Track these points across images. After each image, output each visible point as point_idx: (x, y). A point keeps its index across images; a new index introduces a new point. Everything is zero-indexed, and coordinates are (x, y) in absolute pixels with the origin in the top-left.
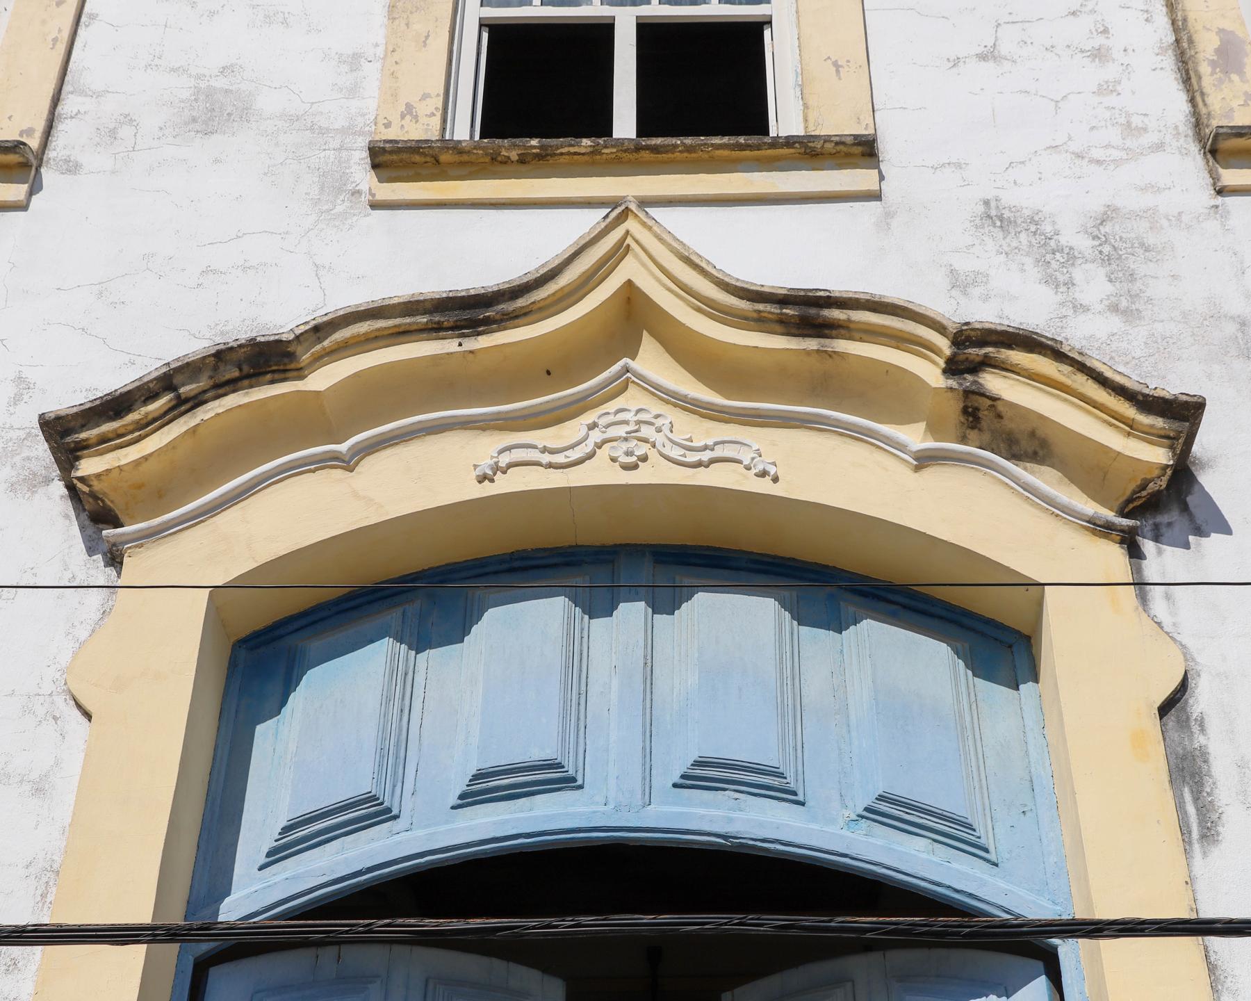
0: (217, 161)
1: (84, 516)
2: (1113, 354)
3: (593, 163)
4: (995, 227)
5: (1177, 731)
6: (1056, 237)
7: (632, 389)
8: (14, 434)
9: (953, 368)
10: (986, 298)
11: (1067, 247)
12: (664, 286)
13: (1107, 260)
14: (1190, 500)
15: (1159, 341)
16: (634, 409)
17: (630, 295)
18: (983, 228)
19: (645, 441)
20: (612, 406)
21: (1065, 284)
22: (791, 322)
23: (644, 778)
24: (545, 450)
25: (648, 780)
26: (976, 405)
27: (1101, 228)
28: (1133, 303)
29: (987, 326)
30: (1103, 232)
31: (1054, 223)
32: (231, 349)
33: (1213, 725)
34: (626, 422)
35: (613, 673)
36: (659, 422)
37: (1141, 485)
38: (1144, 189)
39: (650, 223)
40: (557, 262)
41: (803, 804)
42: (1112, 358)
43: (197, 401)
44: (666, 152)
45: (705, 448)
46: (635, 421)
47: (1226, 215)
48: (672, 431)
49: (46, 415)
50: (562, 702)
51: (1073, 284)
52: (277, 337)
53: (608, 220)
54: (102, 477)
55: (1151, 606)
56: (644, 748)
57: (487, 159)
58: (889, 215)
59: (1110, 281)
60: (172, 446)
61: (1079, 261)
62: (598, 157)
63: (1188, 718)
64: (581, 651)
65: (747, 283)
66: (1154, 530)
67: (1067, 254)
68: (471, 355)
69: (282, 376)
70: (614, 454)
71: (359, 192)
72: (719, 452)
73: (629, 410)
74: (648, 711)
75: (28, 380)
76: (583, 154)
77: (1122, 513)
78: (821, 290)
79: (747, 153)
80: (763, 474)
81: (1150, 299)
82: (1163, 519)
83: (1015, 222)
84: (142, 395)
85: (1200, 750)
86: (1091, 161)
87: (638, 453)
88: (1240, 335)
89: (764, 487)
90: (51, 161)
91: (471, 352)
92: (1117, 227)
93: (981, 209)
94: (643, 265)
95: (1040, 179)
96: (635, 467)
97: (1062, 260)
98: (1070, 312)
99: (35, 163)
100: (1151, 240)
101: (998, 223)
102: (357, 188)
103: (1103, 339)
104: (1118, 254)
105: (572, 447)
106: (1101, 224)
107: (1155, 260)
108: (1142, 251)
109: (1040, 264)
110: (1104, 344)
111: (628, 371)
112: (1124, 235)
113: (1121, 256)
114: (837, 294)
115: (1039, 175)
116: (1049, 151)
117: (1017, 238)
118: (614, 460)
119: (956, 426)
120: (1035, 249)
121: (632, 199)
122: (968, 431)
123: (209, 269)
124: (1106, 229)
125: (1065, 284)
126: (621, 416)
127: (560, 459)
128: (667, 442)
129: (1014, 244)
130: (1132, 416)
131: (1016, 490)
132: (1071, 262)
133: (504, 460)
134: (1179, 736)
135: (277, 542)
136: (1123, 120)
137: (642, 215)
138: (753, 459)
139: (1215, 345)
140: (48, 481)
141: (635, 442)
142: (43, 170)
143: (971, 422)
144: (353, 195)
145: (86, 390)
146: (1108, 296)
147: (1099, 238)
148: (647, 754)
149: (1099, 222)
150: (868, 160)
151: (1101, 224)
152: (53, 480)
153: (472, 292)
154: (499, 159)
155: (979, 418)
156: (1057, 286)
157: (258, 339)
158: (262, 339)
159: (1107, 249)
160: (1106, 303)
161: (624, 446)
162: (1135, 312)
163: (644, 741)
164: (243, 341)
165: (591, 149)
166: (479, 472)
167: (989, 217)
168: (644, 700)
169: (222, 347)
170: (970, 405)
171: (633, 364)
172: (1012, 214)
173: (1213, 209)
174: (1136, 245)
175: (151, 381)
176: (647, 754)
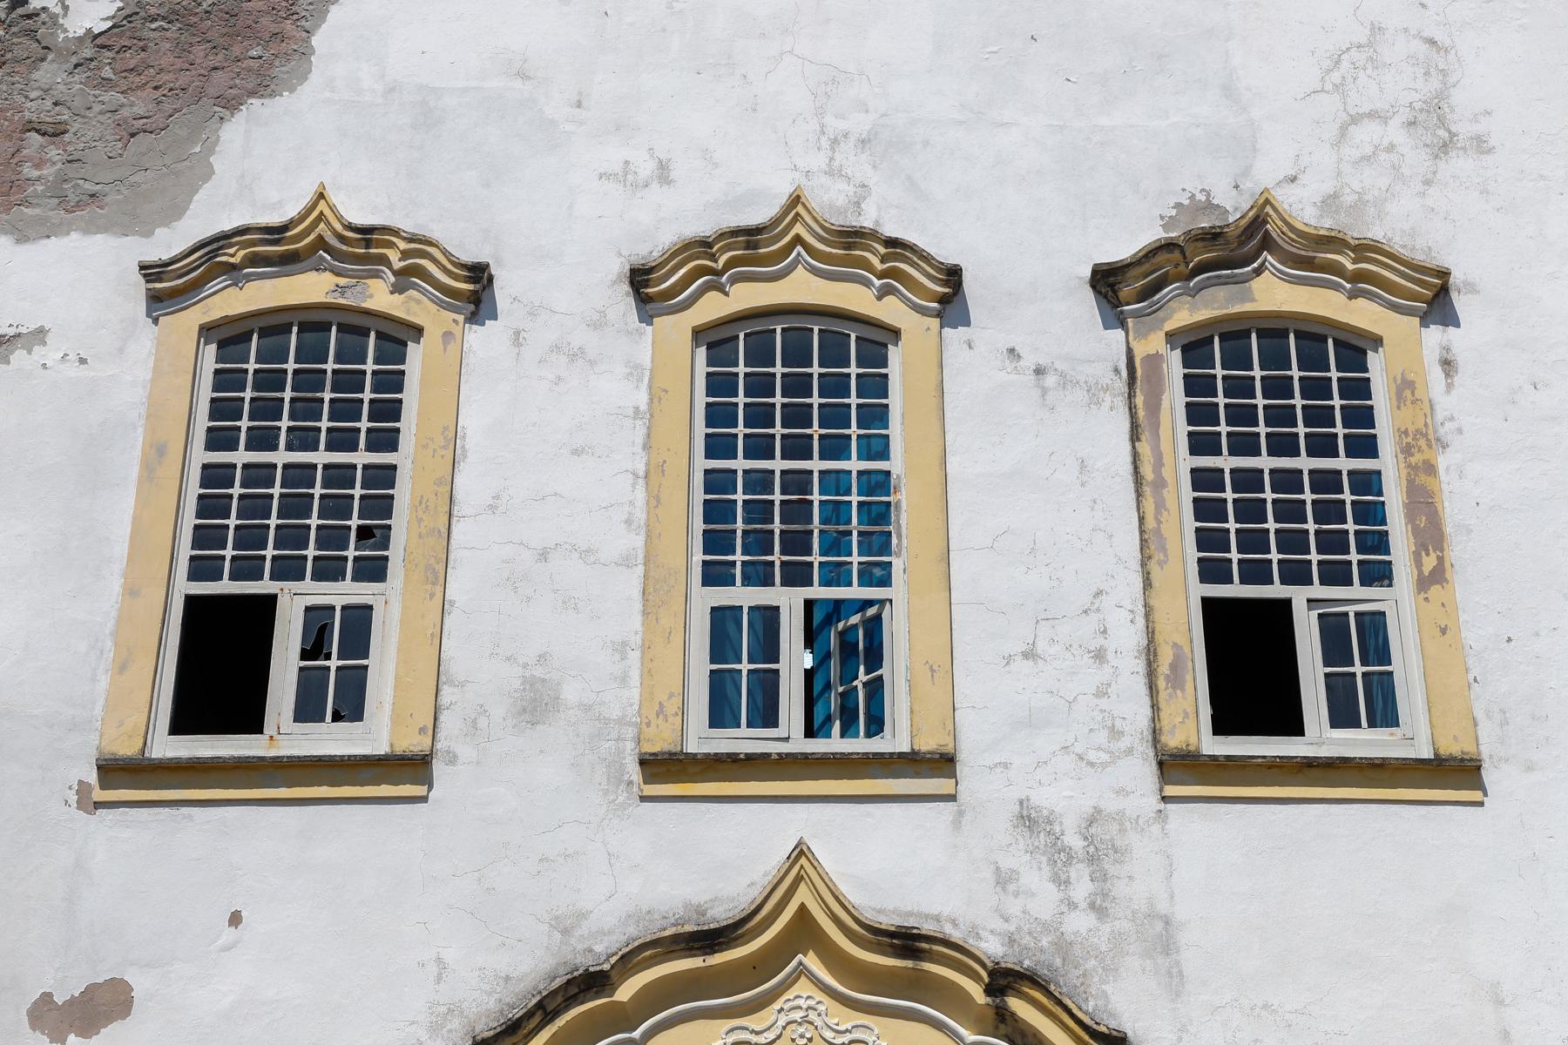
2: (1089, 949)
7: (803, 978)
10: (1016, 895)
12: (823, 909)
13: (1092, 860)
16: (805, 996)
20: (789, 995)
24: (753, 1032)
28: (1104, 901)
34: (800, 1007)
36: (822, 1008)
45: (847, 1031)
51: (1070, 883)
58: (961, 813)
70: (794, 1037)
73: (802, 997)
87: (808, 1035)
94: (811, 891)
97: (1064, 860)
98: (1065, 909)
100: (1118, 843)
101: (1027, 824)
105: (769, 1028)
113: (1099, 856)
124: (1093, 830)
128: (825, 1027)
129: (1036, 844)
136: (1109, 723)
138: (874, 1042)
146: (1089, 894)
147: (1088, 839)
149: (1088, 823)
160: (1088, 900)
161: (801, 1030)
162: (1105, 910)
167: (1022, 817)
171: (806, 961)
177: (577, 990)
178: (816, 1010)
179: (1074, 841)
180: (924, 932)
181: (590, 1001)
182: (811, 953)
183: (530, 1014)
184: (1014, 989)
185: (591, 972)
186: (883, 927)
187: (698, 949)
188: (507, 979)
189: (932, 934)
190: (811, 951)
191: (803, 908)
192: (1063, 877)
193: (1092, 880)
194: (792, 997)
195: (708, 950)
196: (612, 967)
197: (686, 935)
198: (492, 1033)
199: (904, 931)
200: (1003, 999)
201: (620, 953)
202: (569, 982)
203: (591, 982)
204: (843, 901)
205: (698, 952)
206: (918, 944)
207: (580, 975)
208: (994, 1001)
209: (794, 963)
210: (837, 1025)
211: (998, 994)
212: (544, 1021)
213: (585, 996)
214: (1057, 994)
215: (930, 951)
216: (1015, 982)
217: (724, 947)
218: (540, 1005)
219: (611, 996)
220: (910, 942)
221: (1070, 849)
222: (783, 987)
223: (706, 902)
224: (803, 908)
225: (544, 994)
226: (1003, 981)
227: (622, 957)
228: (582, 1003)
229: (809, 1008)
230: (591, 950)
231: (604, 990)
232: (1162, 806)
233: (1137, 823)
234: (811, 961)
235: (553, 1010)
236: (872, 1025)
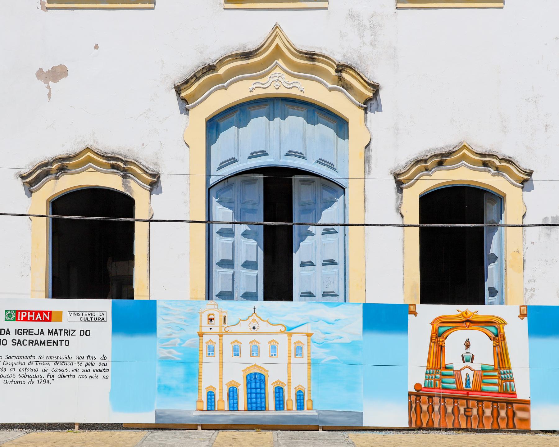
9: (337, 71)
13: (372, 29)
14: (378, 97)
16: (278, 73)
20: (273, 72)
36: (282, 76)
41: (306, 159)
45: (291, 84)
61: (366, 29)
80: (301, 91)
82: (372, 102)
89: (301, 94)
94: (280, 39)
96: (278, 88)
118: (274, 86)
124: (372, 19)
125: (363, 36)
127: (264, 86)
133: (255, 86)
161: (277, 83)
167: (350, 15)
177: (206, 71)
178: (281, 77)
179: (367, 23)
180: (316, 53)
181: (210, 74)
182: (280, 60)
183: (192, 78)
184: (344, 71)
186: (303, 51)
187: (244, 58)
188: (184, 67)
189: (319, 53)
190: (280, 59)
191: (277, 45)
192: (362, 35)
193: (371, 36)
194: (274, 73)
195: (247, 58)
196: (217, 63)
198: (180, 83)
199: (310, 52)
200: (341, 74)
201: (219, 59)
202: (203, 68)
203: (211, 68)
204: (290, 43)
205: (244, 59)
206: (314, 56)
207: (207, 66)
208: (338, 74)
209: (275, 63)
210: (288, 82)
211: (339, 72)
214: (358, 72)
215: (318, 59)
218: (195, 75)
220: (312, 56)
221: (365, 25)
222: (271, 70)
223: (246, 43)
224: (277, 45)
225: (196, 72)
226: (341, 68)
227: (220, 60)
228: (208, 75)
229: (279, 77)
230: (210, 58)
232: (396, 10)
233: (387, 17)
234: (280, 62)
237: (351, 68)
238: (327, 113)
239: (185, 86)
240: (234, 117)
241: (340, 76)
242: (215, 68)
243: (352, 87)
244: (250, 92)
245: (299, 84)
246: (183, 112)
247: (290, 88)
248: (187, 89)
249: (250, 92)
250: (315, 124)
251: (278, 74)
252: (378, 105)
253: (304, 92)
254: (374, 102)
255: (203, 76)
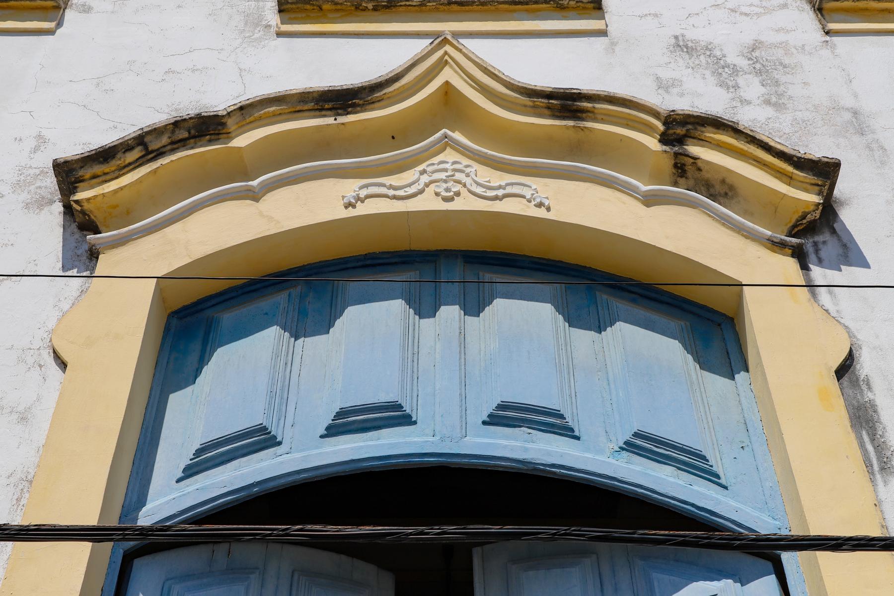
0: (179, 7)
1: (74, 226)
2: (771, 131)
3: (421, 11)
4: (683, 52)
5: (851, 389)
6: (724, 58)
7: (448, 150)
8: (32, 172)
10: (682, 95)
11: (731, 64)
13: (759, 73)
15: (801, 123)
16: (451, 161)
17: (448, 89)
18: (676, 52)
19: (459, 182)
20: (435, 160)
21: (733, 87)
22: (555, 109)
23: (461, 417)
24: (391, 187)
25: (464, 418)
26: (683, 162)
27: (753, 53)
29: (687, 112)
30: (754, 56)
31: (721, 50)
32: (185, 120)
33: (876, 383)
34: (446, 170)
35: (437, 340)
36: (468, 170)
37: (802, 216)
38: (778, 31)
39: (460, 47)
40: (400, 70)
42: (770, 133)
43: (160, 154)
44: (468, 5)
46: (452, 169)
47: (834, 47)
48: (476, 176)
49: (58, 160)
50: (401, 359)
51: (739, 87)
52: (215, 113)
53: (433, 45)
54: (91, 201)
55: (819, 298)
56: (461, 395)
57: (353, 8)
58: (613, 44)
59: (763, 85)
60: (140, 181)
62: (424, 8)
63: (857, 380)
64: (414, 323)
65: (526, 84)
66: (814, 246)
67: (733, 68)
68: (343, 126)
69: (216, 137)
70: (438, 190)
71: (270, 26)
72: (509, 190)
74: (463, 367)
75: (45, 137)
76: (415, 6)
77: (790, 235)
78: (574, 89)
79: (520, 6)
81: (790, 98)
82: (819, 238)
83: (696, 49)
84: (124, 148)
85: (870, 403)
86: (741, 14)
87: (454, 190)
88: (854, 120)
89: (541, 213)
90: (74, 6)
91: (343, 124)
92: (763, 53)
93: (673, 41)
95: (709, 24)
97: (730, 73)
98: (739, 104)
99: (63, 6)
100: (786, 61)
101: (685, 50)
102: (269, 24)
103: (763, 121)
104: (766, 69)
105: (410, 185)
106: (753, 51)
107: (791, 73)
108: (781, 68)
109: (715, 74)
110: (764, 125)
111: (446, 137)
112: (768, 58)
114: (585, 92)
115: (709, 22)
116: (713, 8)
117: (699, 59)
118: (437, 194)
119: (670, 175)
120: (711, 66)
121: (448, 33)
122: (678, 179)
123: (170, 70)
124: (757, 53)
126: (442, 166)
129: (697, 62)
130: (792, 171)
131: (715, 218)
132: (736, 74)
133: (363, 193)
134: (853, 392)
135: (206, 245)
137: (455, 42)
139: (838, 126)
140: (51, 202)
141: (452, 183)
142: (66, 11)
143: (680, 173)
144: (265, 27)
145: (83, 144)
147: (752, 60)
148: (464, 398)
149: (751, 49)
150: (596, 13)
151: (753, 51)
152: (55, 201)
153: (345, 87)
154: (361, 8)
155: (685, 170)
156: (728, 88)
157: (203, 114)
158: (206, 114)
159: (758, 66)
160: (762, 99)
163: (460, 389)
164: (193, 116)
165: (420, 3)
166: (346, 200)
168: (460, 358)
169: (178, 119)
170: (679, 162)
172: (694, 44)
173: (825, 43)
174: (777, 64)
175: (130, 139)
176: (464, 398)
177: (186, 135)
181: (201, 146)
183: (125, 146)
184: (694, 138)
185: (204, 116)
187: (330, 109)
195: (340, 111)
197: (315, 95)
205: (329, 113)
210: (489, 182)
212: (144, 159)
213: (196, 143)
216: (696, 129)
217: (359, 109)
219: (227, 144)
222: (426, 154)
228: (192, 148)
231: (219, 139)
232: (828, 38)
235: (158, 150)
236: (528, 183)
237: (718, 124)
238: (641, 296)
239: (98, 169)
240: (280, 299)
241: (681, 154)
242: (220, 127)
243: (732, 188)
244: (346, 207)
245: (531, 187)
246: (77, 263)
247: (496, 198)
248: (101, 179)
249: (346, 207)
250: (599, 327)
251: (450, 164)
252: (845, 246)
253: (548, 209)
254: (824, 236)
255: (173, 151)
